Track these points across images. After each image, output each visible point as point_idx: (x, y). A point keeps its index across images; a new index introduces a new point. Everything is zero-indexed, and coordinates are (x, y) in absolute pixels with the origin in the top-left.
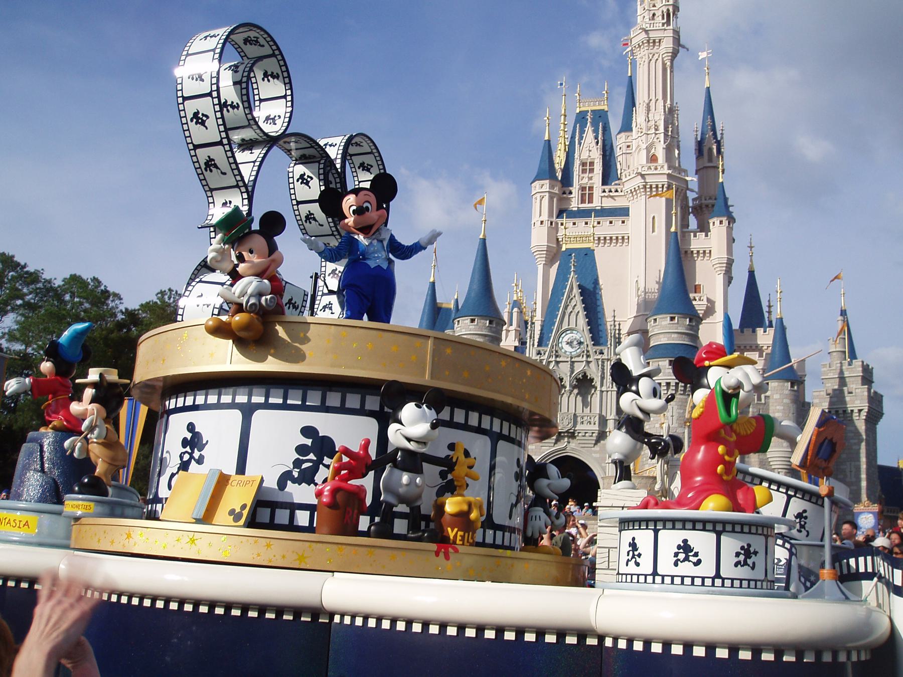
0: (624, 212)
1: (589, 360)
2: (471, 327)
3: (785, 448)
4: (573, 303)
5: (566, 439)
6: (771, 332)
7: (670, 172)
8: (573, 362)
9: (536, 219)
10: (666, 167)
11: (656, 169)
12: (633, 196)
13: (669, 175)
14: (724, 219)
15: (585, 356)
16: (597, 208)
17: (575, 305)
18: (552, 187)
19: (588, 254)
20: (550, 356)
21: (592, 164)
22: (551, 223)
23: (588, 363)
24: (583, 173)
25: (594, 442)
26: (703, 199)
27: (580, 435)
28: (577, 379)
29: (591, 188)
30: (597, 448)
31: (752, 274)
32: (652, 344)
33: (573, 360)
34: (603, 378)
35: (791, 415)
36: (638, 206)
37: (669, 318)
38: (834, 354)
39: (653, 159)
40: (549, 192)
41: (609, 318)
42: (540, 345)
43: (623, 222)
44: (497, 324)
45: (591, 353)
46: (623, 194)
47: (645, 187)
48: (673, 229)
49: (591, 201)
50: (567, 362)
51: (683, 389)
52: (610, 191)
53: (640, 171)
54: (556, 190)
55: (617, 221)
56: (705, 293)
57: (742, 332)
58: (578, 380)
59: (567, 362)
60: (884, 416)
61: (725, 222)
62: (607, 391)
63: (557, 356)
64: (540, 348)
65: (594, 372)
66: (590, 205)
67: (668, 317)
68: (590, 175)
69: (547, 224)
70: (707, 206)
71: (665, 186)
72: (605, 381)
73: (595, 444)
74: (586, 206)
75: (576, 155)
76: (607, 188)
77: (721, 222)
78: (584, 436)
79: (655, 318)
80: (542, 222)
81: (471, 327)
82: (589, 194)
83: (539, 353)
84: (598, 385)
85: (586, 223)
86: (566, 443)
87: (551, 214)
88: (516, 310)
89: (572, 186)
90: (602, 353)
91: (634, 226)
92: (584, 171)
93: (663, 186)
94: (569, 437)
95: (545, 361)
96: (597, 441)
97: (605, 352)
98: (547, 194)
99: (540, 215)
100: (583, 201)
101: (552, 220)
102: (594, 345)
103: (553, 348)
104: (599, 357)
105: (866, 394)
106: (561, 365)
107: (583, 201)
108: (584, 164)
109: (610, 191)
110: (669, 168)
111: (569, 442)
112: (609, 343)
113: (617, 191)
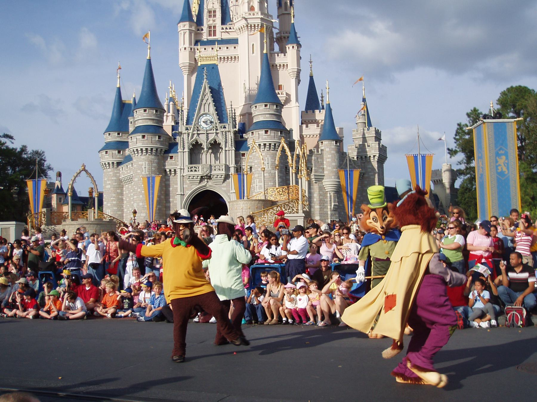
0: (235, 41)
1: (217, 132)
2: (144, 115)
3: (333, 179)
4: (206, 98)
5: (206, 180)
6: (323, 112)
7: (262, 16)
8: (208, 134)
9: (181, 46)
10: (260, 13)
11: (254, 15)
12: (240, 31)
13: (262, 19)
14: (295, 46)
15: (215, 130)
16: (219, 39)
17: (208, 99)
18: (190, 26)
19: (213, 69)
20: (194, 131)
21: (215, 12)
22: (191, 49)
23: (217, 133)
24: (209, 17)
25: (222, 181)
26: (282, 33)
27: (214, 177)
28: (210, 144)
29: (215, 27)
30: (225, 184)
31: (311, 78)
32: (255, 121)
33: (208, 132)
34: (226, 143)
35: (336, 160)
36: (243, 38)
37: (264, 106)
38: (360, 124)
39: (252, 9)
40: (189, 29)
41: (228, 106)
42: (187, 124)
43: (235, 48)
44: (161, 112)
45: (218, 128)
46: (234, 30)
47: (247, 26)
48: (265, 52)
49: (215, 35)
51: (273, 147)
52: (227, 29)
53: (244, 16)
54: (193, 28)
55: (231, 47)
56: (285, 90)
57: (307, 112)
58: (211, 144)
60: (388, 159)
61: (296, 47)
62: (229, 150)
63: (198, 130)
64: (187, 126)
65: (220, 139)
66: (215, 37)
67: (263, 104)
68: (214, 19)
69: (188, 49)
70: (284, 37)
71: (260, 25)
72: (227, 144)
73: (223, 182)
74: (212, 38)
75: (205, 6)
76: (224, 27)
77: (293, 47)
79: (255, 105)
80: (185, 48)
81: (144, 115)
82: (213, 30)
83: (187, 129)
84: (223, 147)
85: (213, 49)
87: (190, 44)
88: (171, 103)
89: (203, 25)
90: (225, 127)
91: (242, 50)
92: (210, 16)
93: (258, 25)
94: (207, 179)
96: (225, 180)
97: (227, 127)
98: (188, 31)
99: (184, 44)
100: (210, 35)
101: (191, 47)
102: (220, 123)
104: (223, 130)
105: (377, 146)
106: (200, 136)
107: (210, 35)
108: (210, 12)
109: (227, 29)
110: (262, 14)
111: (208, 182)
112: (229, 121)
113: (230, 28)
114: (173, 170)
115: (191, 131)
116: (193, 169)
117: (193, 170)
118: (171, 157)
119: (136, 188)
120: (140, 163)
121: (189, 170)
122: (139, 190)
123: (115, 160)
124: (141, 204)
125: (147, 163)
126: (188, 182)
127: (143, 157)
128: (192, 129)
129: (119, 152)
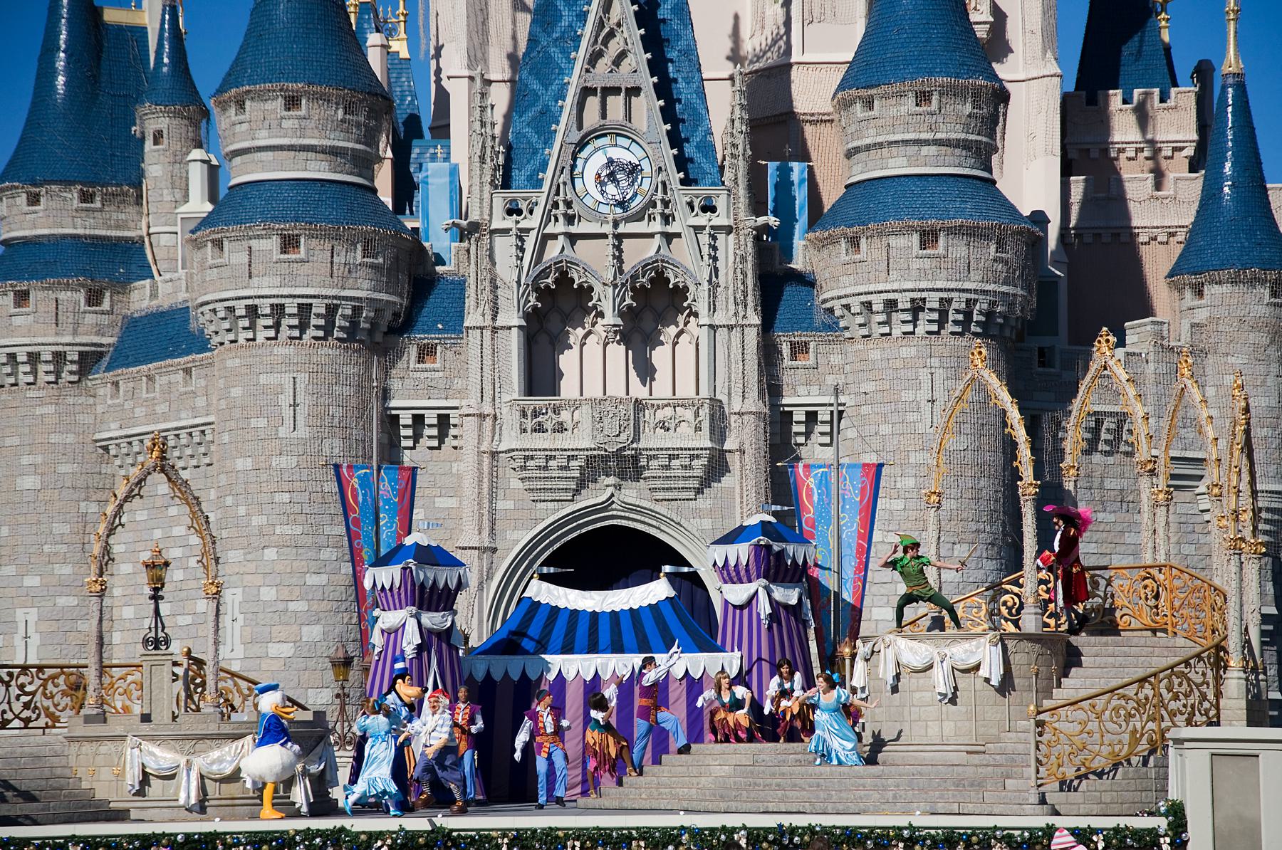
4: (615, 47)
17: (622, 55)
20: (548, 218)
23: (669, 237)
25: (695, 484)
27: (653, 463)
30: (704, 502)
33: (622, 229)
34: (713, 286)
50: (604, 236)
58: (639, 293)
59: (604, 236)
63: (570, 220)
73: (699, 491)
78: (668, 467)
84: (702, 307)
86: (610, 490)
95: (533, 234)
97: (721, 203)
103: (557, 194)
104: (702, 219)
111: (618, 487)
114: (431, 418)
115: (533, 222)
116: (548, 421)
117: (548, 426)
118: (426, 352)
119: (242, 511)
120: (263, 379)
121: (529, 424)
122: (256, 521)
123: (72, 340)
124: (268, 594)
125: (303, 378)
126: (516, 484)
127: (282, 350)
128: (538, 211)
129: (94, 298)
